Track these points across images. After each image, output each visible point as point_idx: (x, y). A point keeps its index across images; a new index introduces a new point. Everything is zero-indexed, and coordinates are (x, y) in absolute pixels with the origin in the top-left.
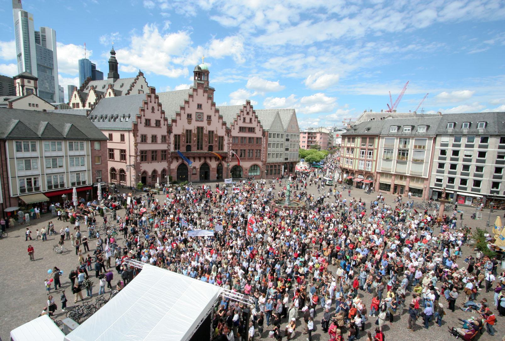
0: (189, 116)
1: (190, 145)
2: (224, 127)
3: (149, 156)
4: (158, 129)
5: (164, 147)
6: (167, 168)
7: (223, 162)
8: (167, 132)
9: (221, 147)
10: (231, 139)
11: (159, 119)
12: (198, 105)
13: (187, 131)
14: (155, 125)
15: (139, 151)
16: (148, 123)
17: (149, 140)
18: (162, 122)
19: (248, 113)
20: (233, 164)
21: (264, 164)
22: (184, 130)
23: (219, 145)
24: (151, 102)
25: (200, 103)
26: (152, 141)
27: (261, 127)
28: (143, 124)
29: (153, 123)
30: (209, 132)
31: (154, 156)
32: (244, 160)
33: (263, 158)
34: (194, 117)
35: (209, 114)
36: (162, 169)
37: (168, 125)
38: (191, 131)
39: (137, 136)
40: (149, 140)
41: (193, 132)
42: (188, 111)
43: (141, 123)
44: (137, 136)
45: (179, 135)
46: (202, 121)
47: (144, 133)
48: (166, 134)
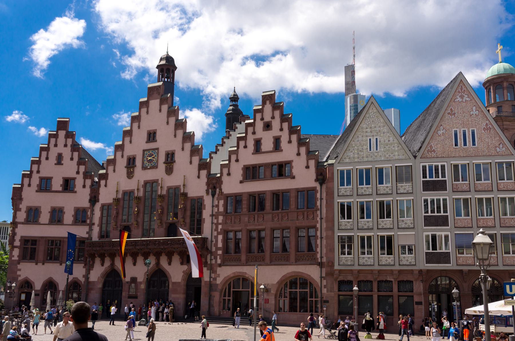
0: (131, 162)
2: (204, 173)
4: (68, 196)
6: (82, 280)
8: (90, 201)
10: (222, 202)
13: (125, 193)
14: (60, 189)
15: (17, 238)
16: (45, 185)
17: (45, 217)
18: (79, 181)
19: (268, 126)
20: (225, 273)
21: (330, 274)
23: (192, 221)
24: (56, 145)
30: (169, 188)
33: (321, 252)
34: (139, 163)
35: (170, 149)
37: (92, 186)
38: (131, 192)
39: (20, 210)
40: (45, 217)
42: (129, 151)
43: (29, 185)
44: (20, 210)
45: (109, 205)
46: (155, 167)
48: (86, 204)
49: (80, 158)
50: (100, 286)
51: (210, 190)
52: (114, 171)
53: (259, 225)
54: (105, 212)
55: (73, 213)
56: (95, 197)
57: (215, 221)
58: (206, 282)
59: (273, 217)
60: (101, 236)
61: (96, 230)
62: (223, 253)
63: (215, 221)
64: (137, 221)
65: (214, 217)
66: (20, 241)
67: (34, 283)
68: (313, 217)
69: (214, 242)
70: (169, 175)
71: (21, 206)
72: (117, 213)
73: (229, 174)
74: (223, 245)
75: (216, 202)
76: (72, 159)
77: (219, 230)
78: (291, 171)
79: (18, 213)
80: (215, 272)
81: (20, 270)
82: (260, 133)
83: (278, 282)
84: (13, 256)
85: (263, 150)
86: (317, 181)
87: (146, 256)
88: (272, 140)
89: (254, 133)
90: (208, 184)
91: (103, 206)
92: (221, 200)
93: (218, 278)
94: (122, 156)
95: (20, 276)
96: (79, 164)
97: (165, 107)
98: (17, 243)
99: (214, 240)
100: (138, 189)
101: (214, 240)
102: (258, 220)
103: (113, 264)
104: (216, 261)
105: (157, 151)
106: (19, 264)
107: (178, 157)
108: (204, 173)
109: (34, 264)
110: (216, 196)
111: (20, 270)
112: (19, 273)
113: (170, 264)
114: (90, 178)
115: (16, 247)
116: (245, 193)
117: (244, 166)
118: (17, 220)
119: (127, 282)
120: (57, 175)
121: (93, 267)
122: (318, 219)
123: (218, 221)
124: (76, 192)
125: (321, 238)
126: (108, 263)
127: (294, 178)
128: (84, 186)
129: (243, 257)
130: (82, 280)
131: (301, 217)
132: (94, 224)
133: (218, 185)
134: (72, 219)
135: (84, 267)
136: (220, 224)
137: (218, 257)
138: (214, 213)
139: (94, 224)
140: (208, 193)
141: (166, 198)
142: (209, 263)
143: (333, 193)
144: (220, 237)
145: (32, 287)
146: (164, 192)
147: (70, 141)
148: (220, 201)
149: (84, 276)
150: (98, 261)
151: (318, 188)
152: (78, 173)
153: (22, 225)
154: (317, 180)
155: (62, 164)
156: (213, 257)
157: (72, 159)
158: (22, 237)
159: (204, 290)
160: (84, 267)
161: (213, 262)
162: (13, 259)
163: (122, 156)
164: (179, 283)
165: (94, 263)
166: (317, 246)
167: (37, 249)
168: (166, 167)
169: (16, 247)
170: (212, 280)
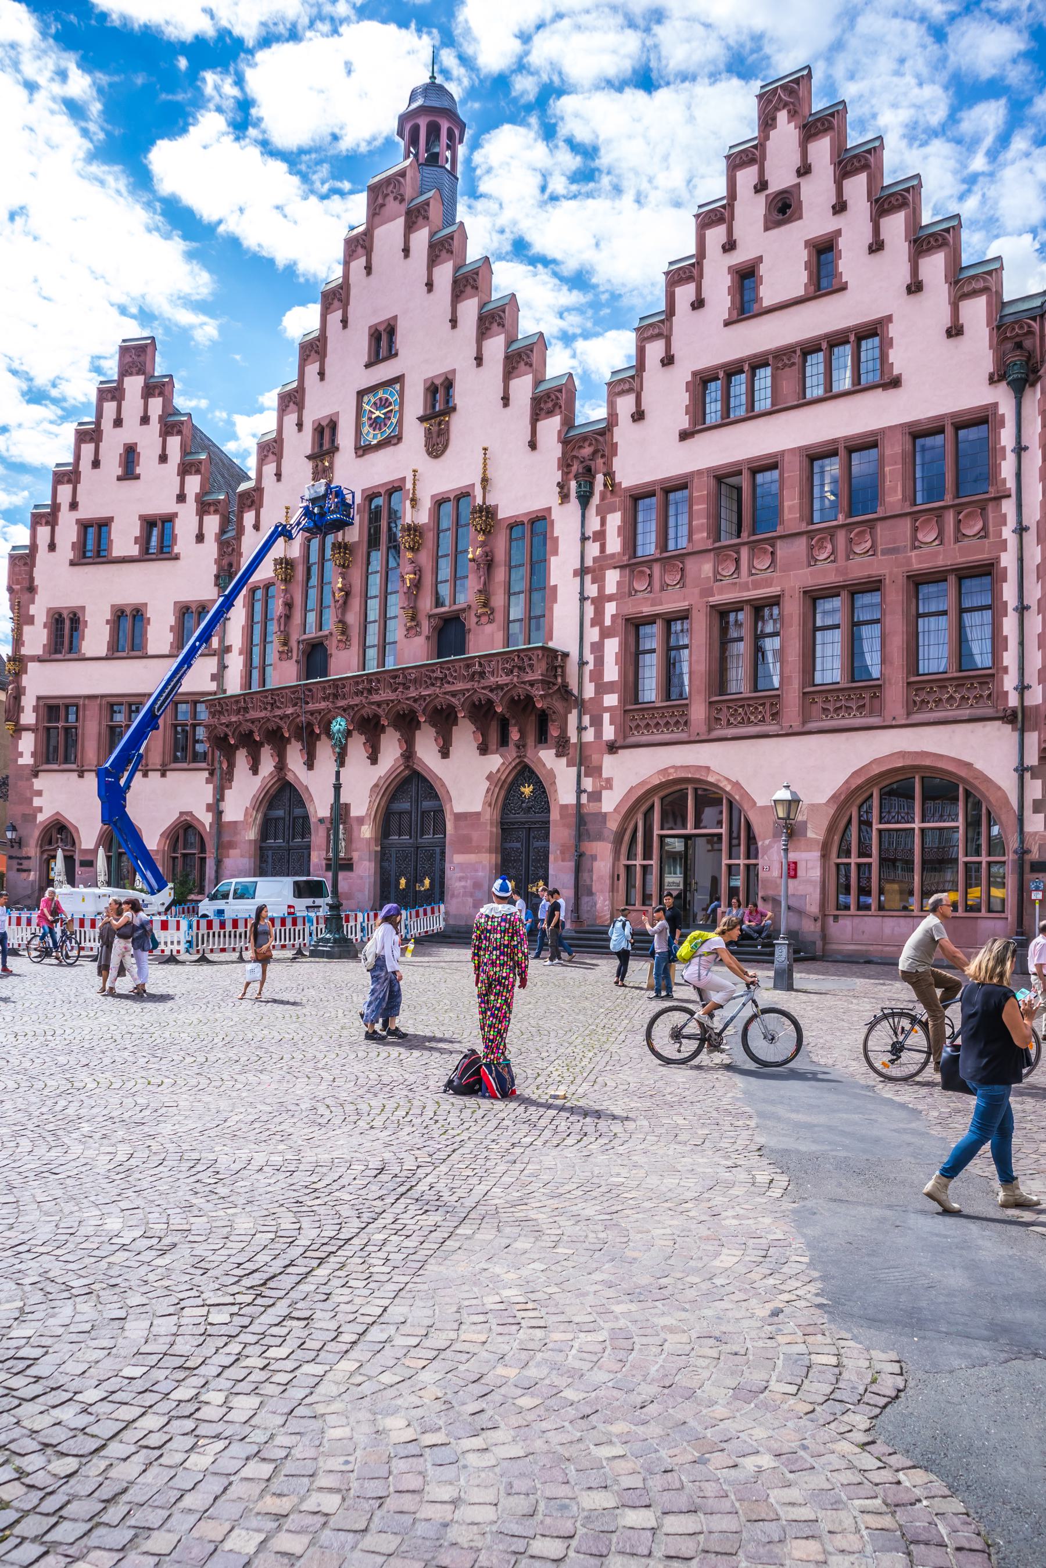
6: (207, 819)
7: (547, 756)
10: (615, 520)
11: (168, 506)
14: (135, 551)
15: (28, 702)
17: (96, 637)
20: (631, 772)
24: (118, 422)
27: (972, 281)
28: (66, 550)
29: (124, 539)
30: (439, 502)
32: (749, 712)
35: (435, 370)
36: (168, 819)
39: (31, 620)
40: (96, 637)
43: (52, 547)
44: (31, 620)
46: (394, 440)
47: (66, 601)
49: (185, 452)
50: (251, 834)
51: (573, 484)
52: (278, 475)
53: (757, 585)
54: (258, 607)
55: (171, 620)
57: (592, 590)
58: (564, 807)
59: (811, 548)
60: (248, 681)
61: (235, 662)
62: (623, 700)
63: (592, 590)
64: (342, 622)
65: (588, 578)
66: (36, 709)
67: (77, 829)
68: (985, 528)
69: (591, 666)
70: (436, 457)
71: (33, 610)
72: (289, 605)
73: (639, 416)
74: (623, 673)
75: (594, 524)
76: (163, 458)
77: (608, 622)
78: (883, 357)
79: (26, 629)
80: (595, 771)
81: (39, 793)
82: (752, 233)
83: (834, 797)
84: (21, 755)
85: (766, 303)
86: (1002, 378)
87: (370, 728)
90: (565, 464)
92: (613, 511)
93: (605, 794)
94: (300, 425)
95: (40, 809)
96: (185, 469)
97: (421, 238)
98: (28, 717)
99: (589, 657)
101: (589, 657)
102: (751, 566)
103: (281, 766)
104: (599, 734)
105: (397, 387)
106: (36, 776)
107: (460, 396)
108: (551, 427)
109: (75, 775)
110: (596, 500)
111: (39, 793)
113: (445, 754)
114: (216, 512)
115: (27, 728)
116: (699, 472)
117: (695, 374)
118: (25, 651)
119: (321, 821)
120: (124, 508)
121: (231, 780)
122: (1008, 533)
123: (601, 589)
124: (177, 558)
125: (1022, 609)
126: (268, 765)
127: (895, 383)
128: (200, 538)
129: (698, 712)
130: (207, 819)
131: (928, 536)
132: (228, 649)
133: (600, 461)
134: (170, 637)
135: (208, 781)
136: (611, 598)
137: (606, 716)
138: (589, 563)
140: (564, 497)
141: (430, 536)
142: (574, 740)
144: (612, 646)
145: (74, 844)
146: (423, 517)
147: (156, 405)
148: (610, 517)
149: (209, 808)
150: (242, 758)
152: (181, 498)
153: (37, 664)
154: (992, 380)
155: (138, 477)
156: (586, 720)
157: (163, 458)
158: (39, 698)
159: (560, 835)
160: (208, 781)
161: (589, 736)
162: (21, 761)
163: (300, 425)
164: (478, 814)
165: (231, 765)
166: (998, 642)
168: (428, 433)
169: (27, 728)
170: (584, 799)
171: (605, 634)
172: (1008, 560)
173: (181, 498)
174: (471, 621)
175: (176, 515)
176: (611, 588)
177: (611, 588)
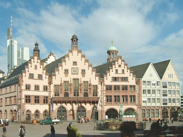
0: (66, 71)
1: (67, 93)
3: (33, 100)
5: (46, 94)
9: (95, 94)
10: (105, 87)
11: (41, 73)
12: (74, 62)
13: (65, 82)
14: (37, 78)
15: (23, 95)
17: (32, 88)
19: (120, 66)
22: (61, 81)
25: (75, 61)
26: (35, 89)
29: (36, 76)
31: (37, 100)
34: (70, 71)
35: (83, 69)
38: (68, 82)
40: (32, 88)
41: (70, 83)
45: (58, 85)
48: (47, 84)
55: (43, 87)
56: (50, 82)
66: (24, 96)
76: (40, 68)
81: (25, 107)
88: (122, 70)
89: (115, 68)
91: (55, 85)
100: (71, 81)
101: (102, 98)
111: (25, 107)
112: (25, 108)
122: (136, 93)
128: (46, 78)
132: (51, 91)
134: (43, 89)
139: (51, 91)
140: (99, 84)
143: (141, 87)
144: (105, 98)
146: (82, 83)
151: (136, 85)
152: (43, 73)
157: (40, 68)
167: (31, 100)
171: (104, 96)
172: (136, 95)
173: (43, 73)
174: (89, 93)
175: (42, 75)
176: (104, 93)
177: (104, 93)
